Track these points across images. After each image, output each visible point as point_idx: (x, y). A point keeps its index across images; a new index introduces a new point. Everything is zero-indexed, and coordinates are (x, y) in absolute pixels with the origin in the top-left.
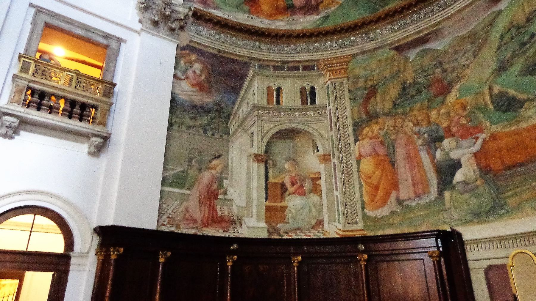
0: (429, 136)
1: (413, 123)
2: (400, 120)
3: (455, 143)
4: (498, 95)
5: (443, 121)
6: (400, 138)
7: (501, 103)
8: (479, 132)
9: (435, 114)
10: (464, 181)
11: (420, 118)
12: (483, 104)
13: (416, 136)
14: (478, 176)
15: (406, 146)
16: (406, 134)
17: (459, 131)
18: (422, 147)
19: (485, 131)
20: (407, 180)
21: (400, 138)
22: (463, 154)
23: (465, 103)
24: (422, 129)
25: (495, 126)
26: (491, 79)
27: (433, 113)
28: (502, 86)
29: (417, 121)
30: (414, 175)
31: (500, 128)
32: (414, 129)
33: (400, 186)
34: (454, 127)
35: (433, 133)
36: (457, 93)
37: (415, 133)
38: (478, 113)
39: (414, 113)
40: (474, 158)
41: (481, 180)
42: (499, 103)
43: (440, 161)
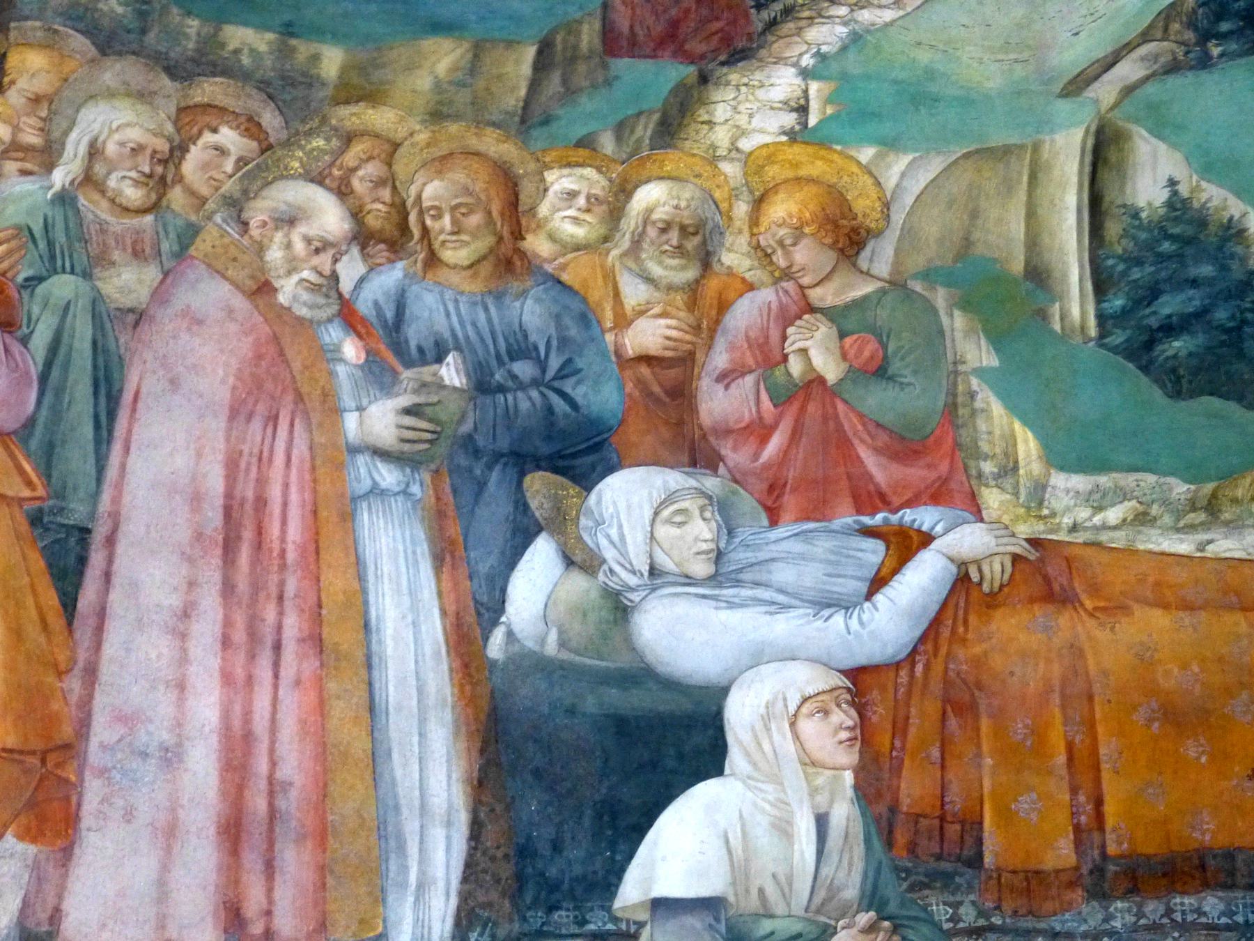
0: (482, 385)
1: (357, 215)
2: (228, 136)
3: (702, 531)
4: (1160, 230)
5: (634, 292)
6: (196, 321)
7: (1170, 305)
8: (937, 495)
9: (581, 201)
10: (708, 905)
11: (433, 190)
12: (1017, 266)
13: (351, 350)
14: (851, 893)
15: (237, 412)
16: (263, 289)
17: (760, 431)
18: (388, 476)
19: (992, 499)
20: (171, 757)
21: (196, 321)
22: (758, 657)
23: (864, 204)
24: (430, 299)
25: (1079, 482)
26: (1128, 70)
27: (560, 181)
28: (1209, 168)
29: (401, 209)
30: (260, 724)
31: (1113, 515)
32: (350, 269)
33: (93, 793)
34: (726, 378)
35: (523, 369)
36: (814, 87)
37: (348, 316)
38: (957, 323)
39: (381, 118)
40: (843, 717)
41: (871, 929)
42: (1154, 293)
43: (541, 666)
